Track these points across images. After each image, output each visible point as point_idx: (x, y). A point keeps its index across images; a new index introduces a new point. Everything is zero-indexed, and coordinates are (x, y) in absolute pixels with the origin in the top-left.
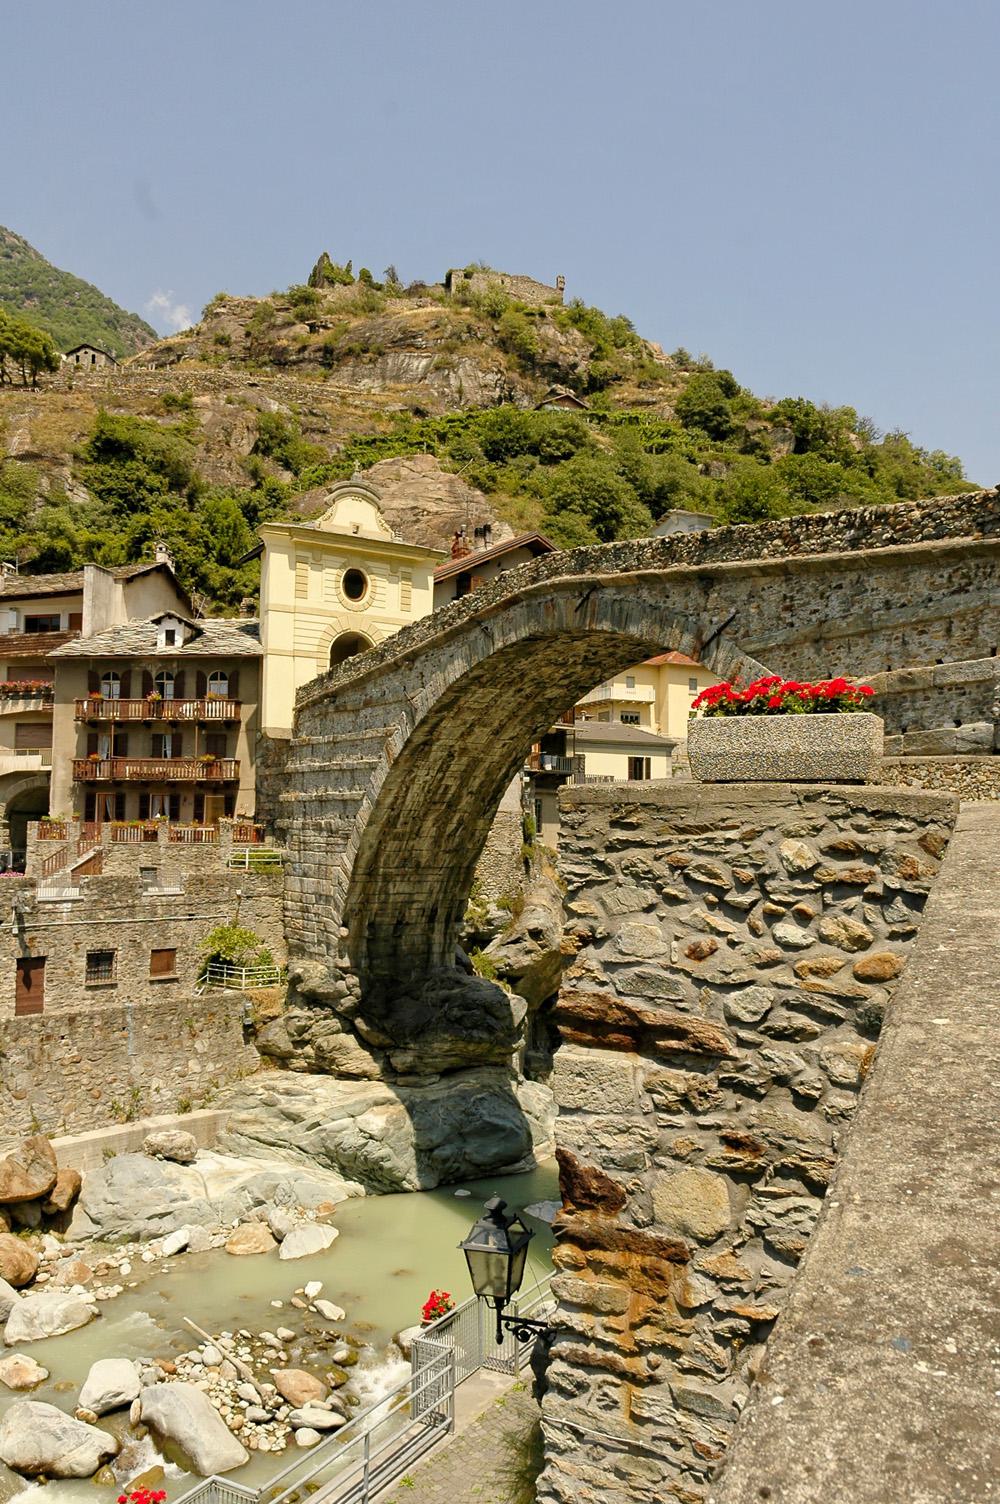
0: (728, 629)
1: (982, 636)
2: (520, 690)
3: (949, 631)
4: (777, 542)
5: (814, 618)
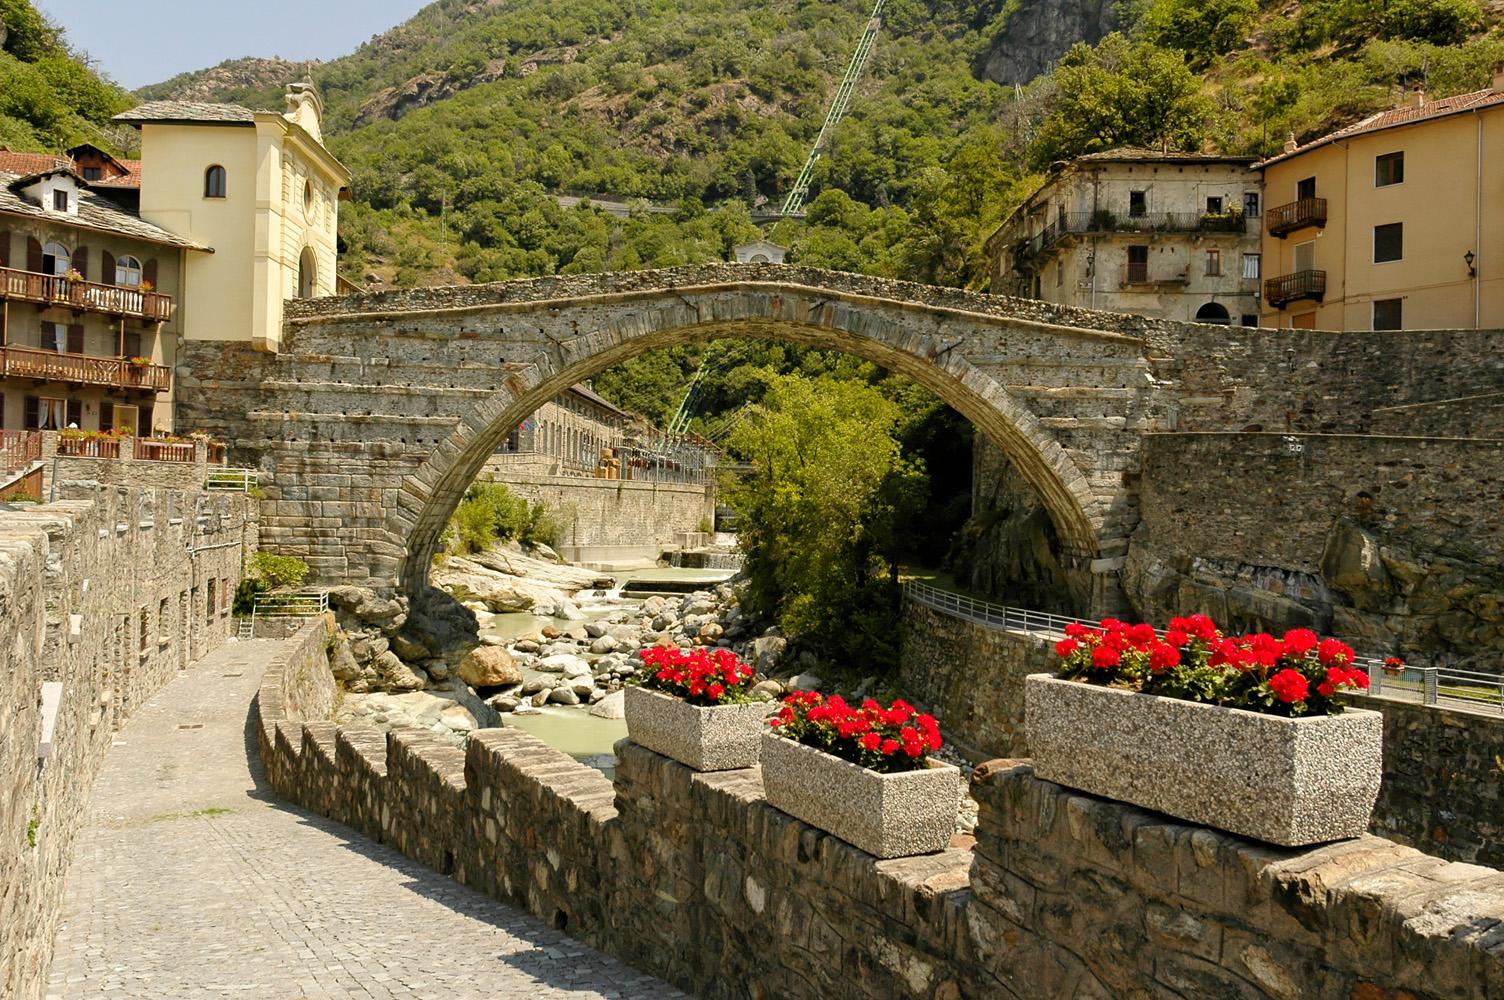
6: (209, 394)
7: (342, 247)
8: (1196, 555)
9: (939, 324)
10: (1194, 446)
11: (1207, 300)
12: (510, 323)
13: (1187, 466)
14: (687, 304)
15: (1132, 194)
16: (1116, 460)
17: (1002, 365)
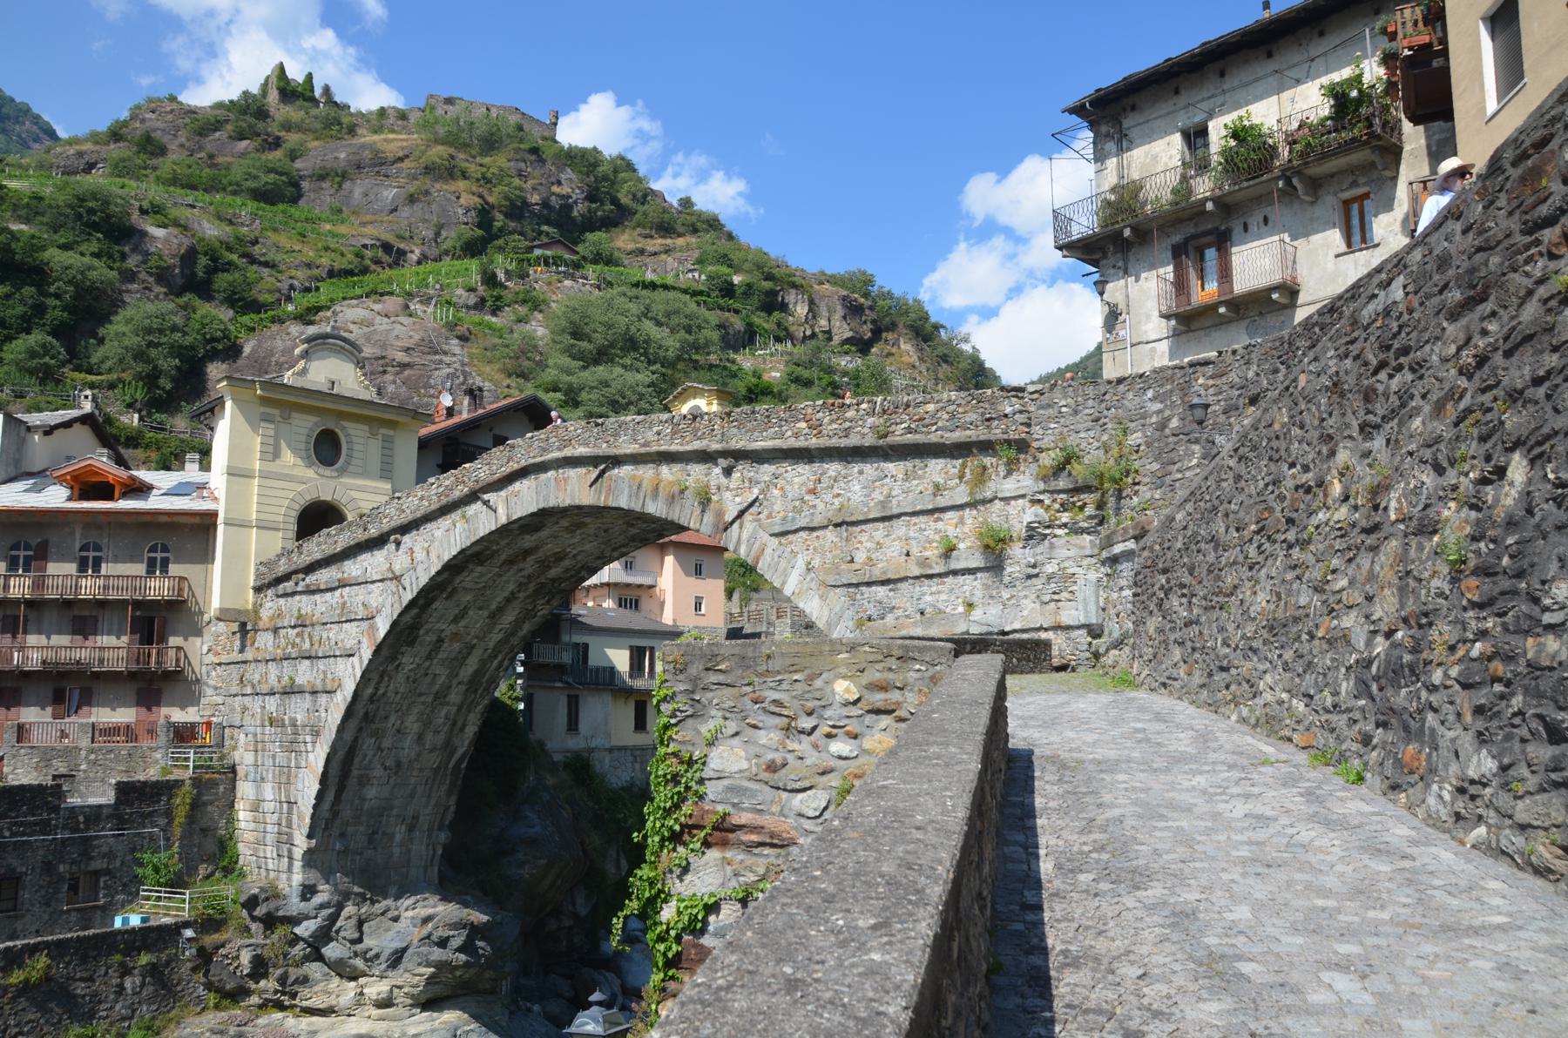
0: (752, 510)
2: (521, 570)
5: (837, 501)
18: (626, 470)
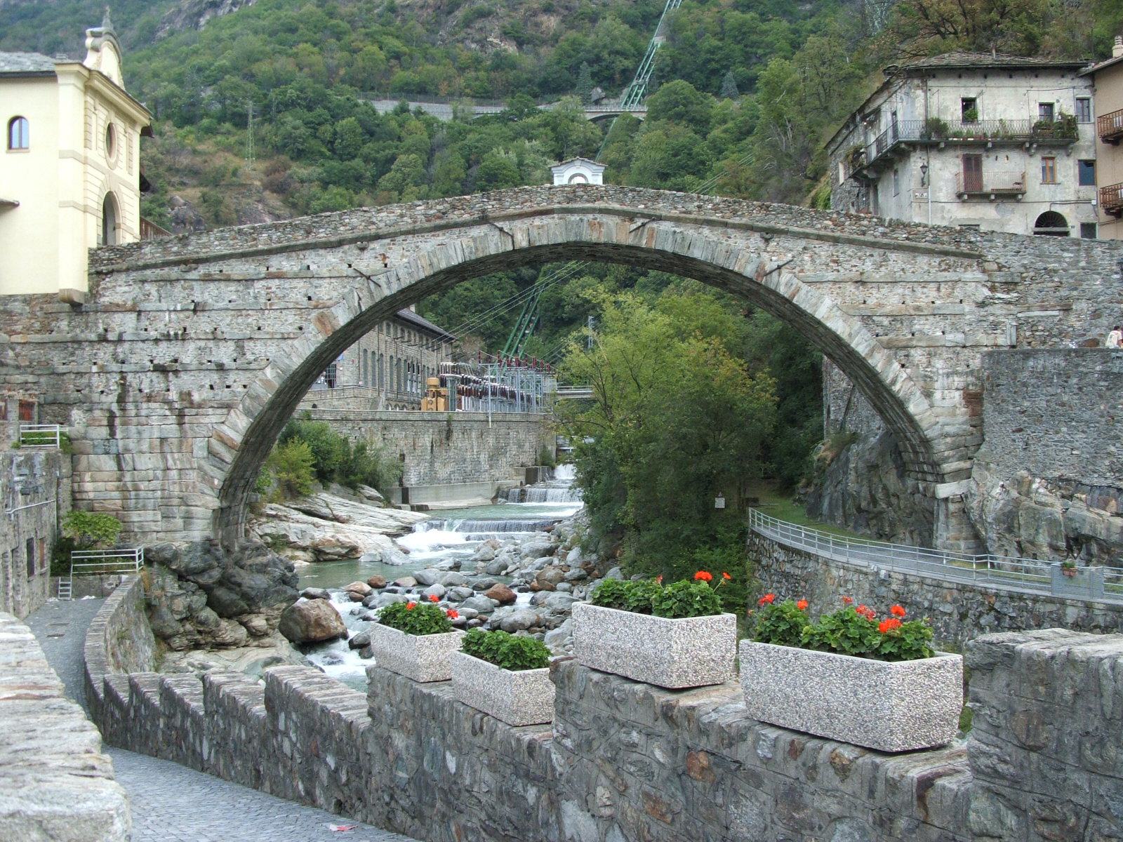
1: (956, 294)
3: (938, 289)
4: (830, 223)
5: (854, 269)
6: (18, 349)
7: (145, 186)
8: (1034, 476)
9: (767, 241)
10: (1031, 363)
11: (1044, 208)
12: (317, 259)
13: (1025, 385)
14: (501, 230)
15: (964, 100)
16: (956, 379)
17: (835, 282)
18: (666, 226)
